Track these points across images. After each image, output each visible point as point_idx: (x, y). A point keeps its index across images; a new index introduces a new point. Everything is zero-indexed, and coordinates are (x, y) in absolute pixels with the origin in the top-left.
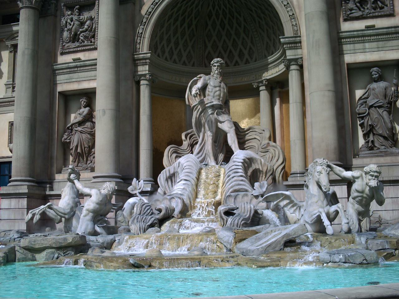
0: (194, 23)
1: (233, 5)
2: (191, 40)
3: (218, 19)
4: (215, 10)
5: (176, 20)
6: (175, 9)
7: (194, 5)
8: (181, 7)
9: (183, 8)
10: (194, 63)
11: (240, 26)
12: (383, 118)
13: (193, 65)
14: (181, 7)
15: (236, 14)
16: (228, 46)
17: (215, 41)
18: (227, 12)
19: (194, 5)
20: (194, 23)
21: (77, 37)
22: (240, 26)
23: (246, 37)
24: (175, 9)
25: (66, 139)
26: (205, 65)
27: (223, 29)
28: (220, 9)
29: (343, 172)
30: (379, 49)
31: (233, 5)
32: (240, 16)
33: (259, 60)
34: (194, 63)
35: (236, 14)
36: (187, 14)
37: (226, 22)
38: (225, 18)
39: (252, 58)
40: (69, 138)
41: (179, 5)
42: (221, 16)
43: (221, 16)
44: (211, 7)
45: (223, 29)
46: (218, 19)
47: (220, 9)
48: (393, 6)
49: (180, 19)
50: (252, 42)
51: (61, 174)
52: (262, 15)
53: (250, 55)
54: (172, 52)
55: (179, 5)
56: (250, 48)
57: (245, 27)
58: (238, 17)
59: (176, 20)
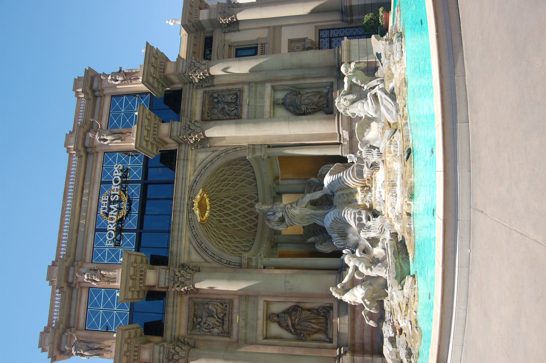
0: (223, 233)
1: (215, 201)
2: (235, 239)
3: (223, 217)
4: (216, 216)
5: (220, 243)
6: (212, 240)
7: (211, 228)
8: (211, 236)
9: (211, 235)
10: (253, 239)
11: (231, 202)
12: (308, 97)
13: (254, 239)
14: (211, 236)
15: (222, 203)
16: (243, 215)
17: (238, 223)
18: (219, 208)
19: (211, 228)
20: (223, 233)
21: (219, 320)
22: (231, 202)
23: (239, 200)
24: (212, 240)
25: (304, 334)
26: (255, 232)
27: (231, 215)
28: (216, 213)
29: (344, 90)
30: (263, 97)
31: (215, 201)
32: (224, 200)
33: (258, 191)
34: (253, 239)
35: (222, 203)
36: (216, 235)
37: (226, 212)
38: (223, 211)
39: (255, 198)
40: (303, 331)
41: (210, 236)
42: (221, 214)
43: (221, 214)
44: (214, 218)
45: (231, 215)
46: (223, 217)
47: (216, 213)
48: (237, 89)
49: (219, 240)
50: (243, 196)
51: (333, 339)
52: (226, 182)
53: (253, 198)
54: (243, 250)
55: (210, 236)
56: (247, 198)
57: (231, 199)
58: (224, 201)
59: (220, 243)
